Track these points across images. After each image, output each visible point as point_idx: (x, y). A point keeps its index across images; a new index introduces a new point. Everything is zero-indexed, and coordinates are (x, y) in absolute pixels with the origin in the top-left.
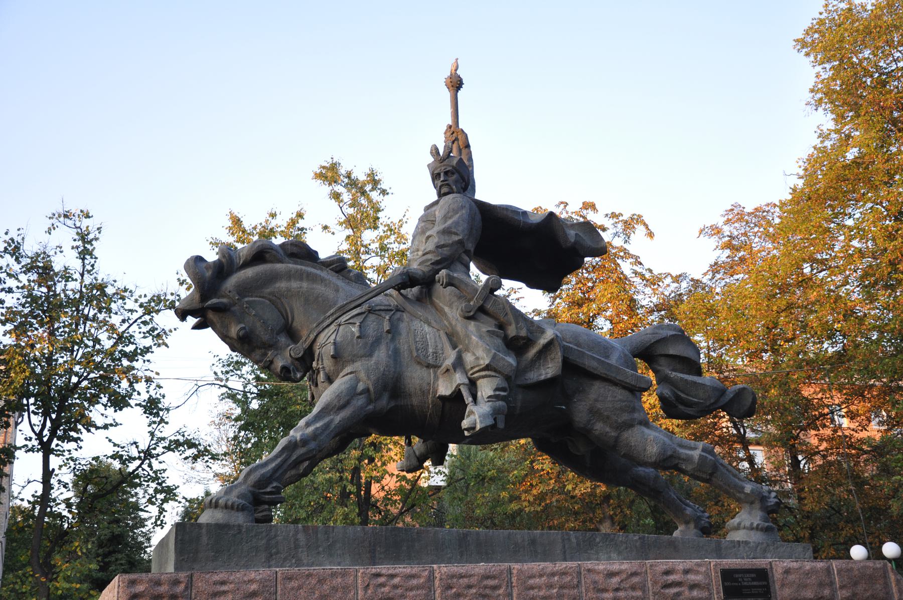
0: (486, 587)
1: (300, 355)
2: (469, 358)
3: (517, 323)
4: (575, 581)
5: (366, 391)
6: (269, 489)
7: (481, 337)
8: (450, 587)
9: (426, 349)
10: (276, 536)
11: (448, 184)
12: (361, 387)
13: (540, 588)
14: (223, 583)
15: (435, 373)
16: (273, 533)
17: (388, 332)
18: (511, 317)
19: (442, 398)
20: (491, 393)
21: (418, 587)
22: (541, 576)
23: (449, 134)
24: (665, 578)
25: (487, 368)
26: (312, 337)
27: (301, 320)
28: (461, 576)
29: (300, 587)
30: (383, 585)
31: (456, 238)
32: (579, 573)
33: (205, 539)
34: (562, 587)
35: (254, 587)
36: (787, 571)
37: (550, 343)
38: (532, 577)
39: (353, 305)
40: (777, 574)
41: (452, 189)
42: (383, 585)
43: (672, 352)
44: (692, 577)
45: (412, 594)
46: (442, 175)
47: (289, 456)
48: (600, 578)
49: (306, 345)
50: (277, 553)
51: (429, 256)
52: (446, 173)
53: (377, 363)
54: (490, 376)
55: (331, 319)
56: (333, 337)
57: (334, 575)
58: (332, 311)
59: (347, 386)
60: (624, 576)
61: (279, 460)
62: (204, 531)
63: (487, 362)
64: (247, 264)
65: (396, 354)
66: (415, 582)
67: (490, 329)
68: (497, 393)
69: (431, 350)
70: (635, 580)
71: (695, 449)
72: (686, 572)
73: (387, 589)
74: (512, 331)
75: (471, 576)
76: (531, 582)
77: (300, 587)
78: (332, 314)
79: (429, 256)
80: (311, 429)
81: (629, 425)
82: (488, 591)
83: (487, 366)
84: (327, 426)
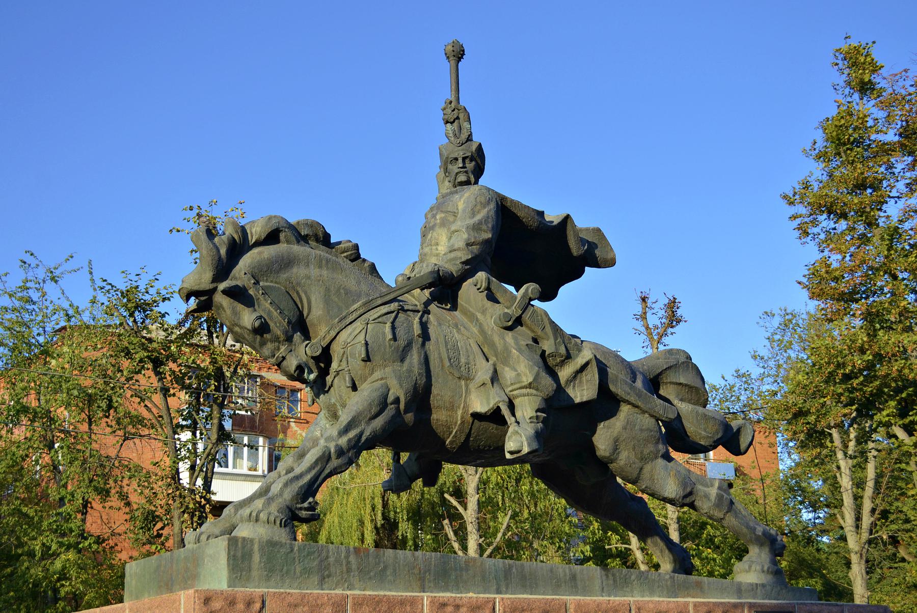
1: (318, 354)
2: (508, 374)
3: (556, 339)
7: (520, 350)
9: (458, 359)
10: (327, 557)
11: (466, 172)
15: (467, 386)
16: (324, 554)
18: (548, 329)
19: (476, 416)
20: (534, 414)
23: (449, 111)
25: (530, 386)
26: (333, 334)
27: (316, 313)
33: (256, 557)
39: (379, 302)
41: (469, 177)
43: (682, 380)
46: (460, 160)
49: (324, 343)
50: (329, 576)
51: (459, 254)
52: (464, 159)
53: (410, 371)
54: (528, 395)
55: (354, 316)
56: (361, 338)
58: (355, 306)
59: (378, 393)
61: (313, 472)
62: (256, 547)
63: (530, 379)
69: (463, 360)
71: (712, 485)
74: (548, 346)
79: (459, 254)
80: (343, 441)
83: (530, 384)
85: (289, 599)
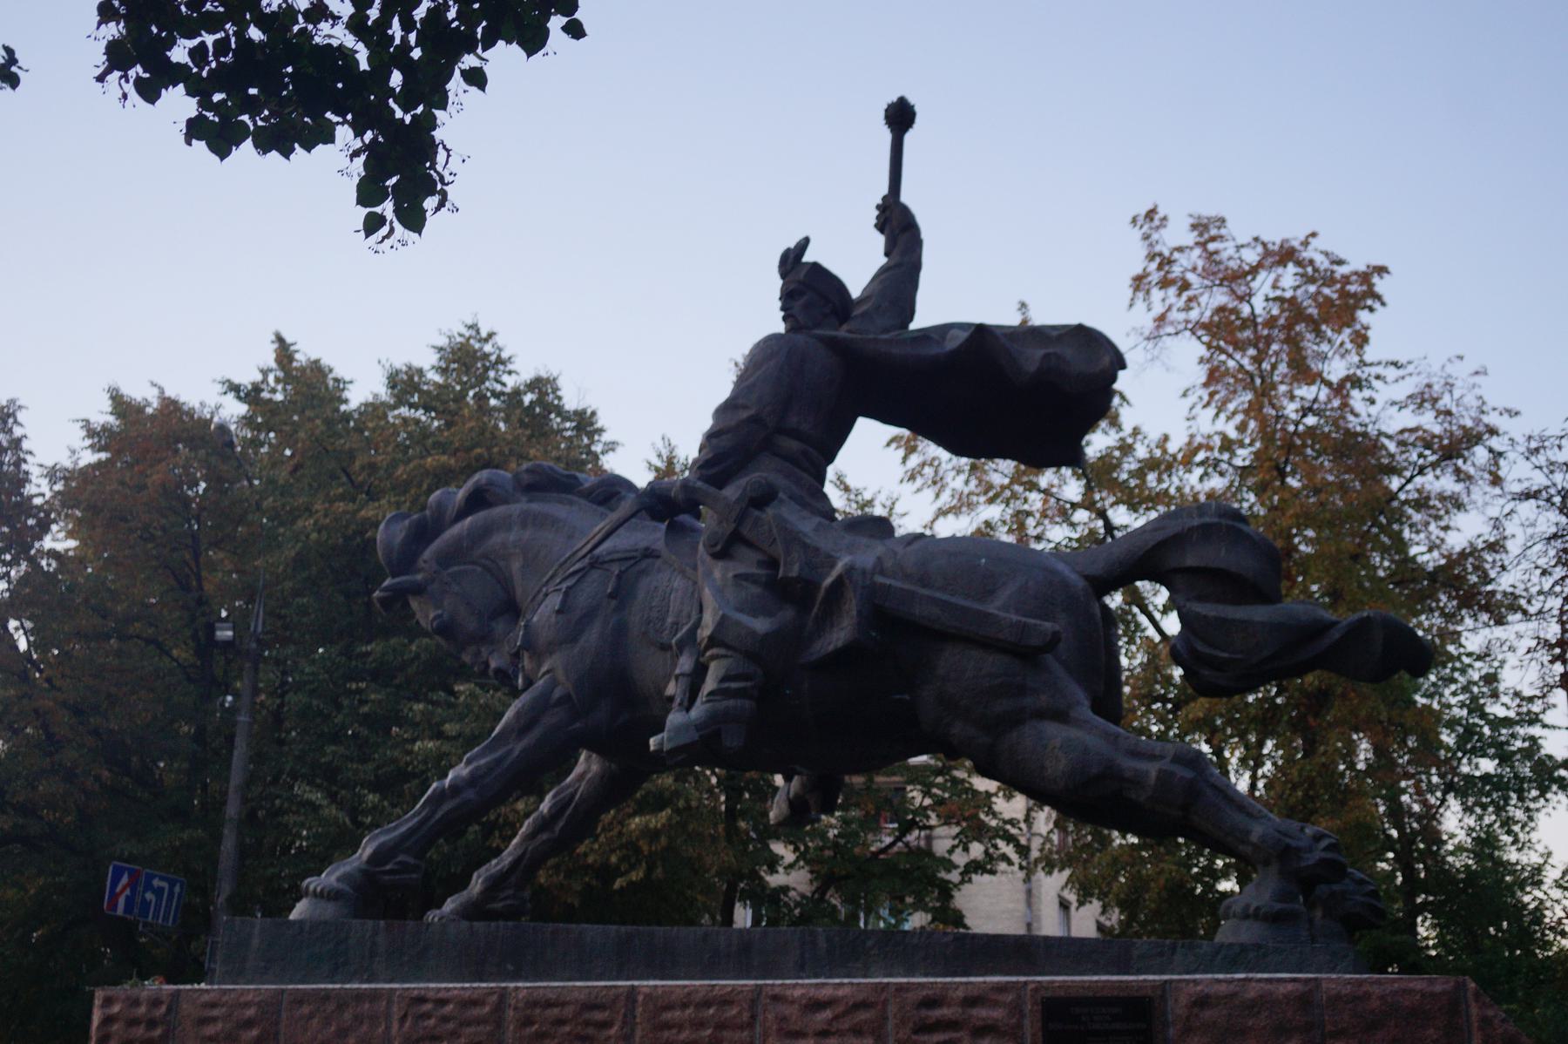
0: (587, 1023)
4: (746, 1016)
5: (566, 698)
6: (388, 867)
8: (528, 1022)
9: (663, 620)
12: (557, 693)
13: (680, 1027)
14: (213, 1005)
17: (612, 596)
21: (479, 1021)
22: (684, 1006)
24: (924, 1012)
28: (549, 1004)
29: (311, 1016)
30: (427, 1016)
31: (744, 415)
32: (753, 1003)
34: (721, 1026)
35: (251, 1012)
36: (1203, 1002)
37: (839, 581)
38: (669, 1007)
40: (1177, 1007)
42: (427, 1016)
44: (981, 1013)
45: (471, 1030)
47: (433, 812)
48: (791, 1011)
57: (359, 996)
60: (840, 1009)
64: (461, 515)
65: (621, 631)
66: (476, 1012)
67: (742, 570)
68: (726, 685)
69: (670, 620)
70: (863, 1016)
72: (972, 1001)
73: (432, 1022)
75: (563, 1004)
76: (667, 1016)
77: (311, 1016)
78: (552, 577)
81: (1016, 719)
82: (590, 1031)
84: (498, 761)
85: (206, 998)
